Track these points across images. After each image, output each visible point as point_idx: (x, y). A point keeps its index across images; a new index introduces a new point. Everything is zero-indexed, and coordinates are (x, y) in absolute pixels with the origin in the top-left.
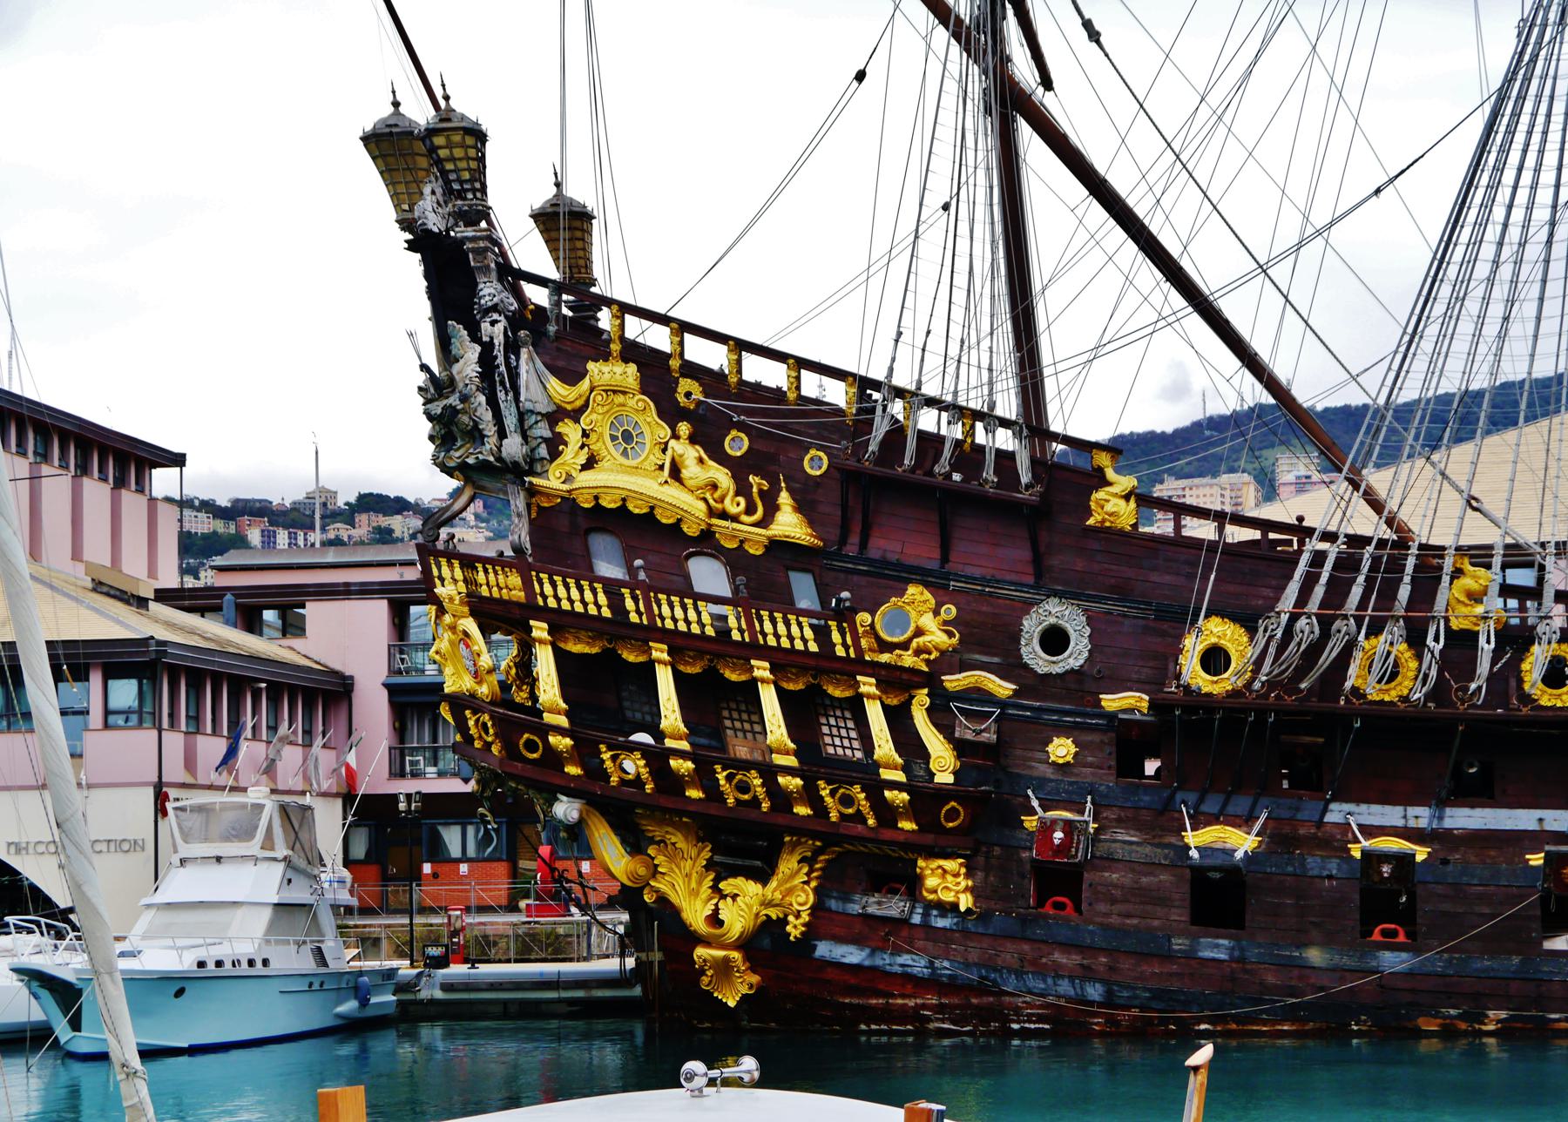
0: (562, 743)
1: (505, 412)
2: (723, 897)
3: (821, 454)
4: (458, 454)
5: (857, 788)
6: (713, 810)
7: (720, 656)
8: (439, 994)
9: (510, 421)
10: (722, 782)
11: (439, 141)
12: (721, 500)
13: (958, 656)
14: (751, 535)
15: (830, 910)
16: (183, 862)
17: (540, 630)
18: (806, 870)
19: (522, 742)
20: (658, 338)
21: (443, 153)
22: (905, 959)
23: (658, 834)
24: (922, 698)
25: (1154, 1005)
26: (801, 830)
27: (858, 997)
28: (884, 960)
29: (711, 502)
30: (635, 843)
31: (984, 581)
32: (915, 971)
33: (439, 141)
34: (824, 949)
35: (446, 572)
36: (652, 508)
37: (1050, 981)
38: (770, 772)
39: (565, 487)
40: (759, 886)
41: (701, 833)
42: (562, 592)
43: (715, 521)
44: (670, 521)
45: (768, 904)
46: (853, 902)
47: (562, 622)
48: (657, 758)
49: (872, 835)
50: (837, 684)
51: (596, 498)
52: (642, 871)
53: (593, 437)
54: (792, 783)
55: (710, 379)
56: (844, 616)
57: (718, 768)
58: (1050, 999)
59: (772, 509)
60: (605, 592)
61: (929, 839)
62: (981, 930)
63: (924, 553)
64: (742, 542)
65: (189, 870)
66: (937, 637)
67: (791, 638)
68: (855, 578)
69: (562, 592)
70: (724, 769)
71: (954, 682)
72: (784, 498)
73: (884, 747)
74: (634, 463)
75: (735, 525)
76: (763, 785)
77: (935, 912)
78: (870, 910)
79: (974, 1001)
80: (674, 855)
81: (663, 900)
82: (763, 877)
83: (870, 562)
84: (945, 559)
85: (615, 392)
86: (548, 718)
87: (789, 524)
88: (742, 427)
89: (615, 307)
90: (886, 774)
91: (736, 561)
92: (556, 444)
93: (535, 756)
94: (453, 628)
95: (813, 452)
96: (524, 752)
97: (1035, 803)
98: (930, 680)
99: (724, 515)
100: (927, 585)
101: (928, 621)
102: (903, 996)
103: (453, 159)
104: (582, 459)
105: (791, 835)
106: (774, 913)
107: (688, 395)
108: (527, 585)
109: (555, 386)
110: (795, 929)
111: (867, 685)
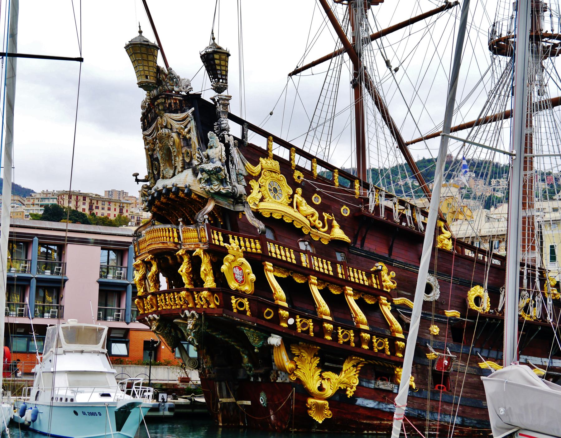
1: (232, 173)
2: (324, 379)
3: (347, 208)
4: (216, 187)
6: (334, 344)
7: (332, 283)
8: (167, 413)
9: (234, 177)
10: (340, 334)
11: (216, 56)
12: (314, 221)
14: (322, 235)
15: (363, 386)
16: (65, 352)
17: (269, 266)
18: (355, 370)
20: (284, 153)
21: (217, 62)
23: (296, 352)
25: (477, 426)
26: (362, 354)
27: (370, 420)
29: (312, 221)
30: (291, 356)
31: (406, 264)
33: (216, 56)
34: (360, 401)
36: (293, 221)
37: (443, 416)
38: (358, 331)
39: (255, 208)
40: (337, 375)
43: (312, 229)
44: (299, 227)
46: (371, 383)
48: (318, 322)
50: (370, 298)
51: (271, 214)
53: (263, 189)
55: (308, 174)
58: (442, 423)
59: (331, 227)
62: (419, 396)
63: (384, 252)
64: (320, 238)
65: (68, 355)
71: (398, 301)
72: (335, 223)
74: (280, 201)
76: (354, 336)
81: (298, 380)
82: (338, 371)
83: (366, 252)
84: (390, 254)
85: (271, 171)
86: (280, 303)
87: (338, 233)
88: (319, 193)
89: (271, 138)
92: (249, 189)
93: (269, 318)
95: (345, 207)
96: (265, 316)
97: (431, 349)
99: (314, 227)
103: (220, 65)
104: (260, 196)
106: (342, 387)
107: (299, 177)
109: (248, 164)
110: (350, 393)
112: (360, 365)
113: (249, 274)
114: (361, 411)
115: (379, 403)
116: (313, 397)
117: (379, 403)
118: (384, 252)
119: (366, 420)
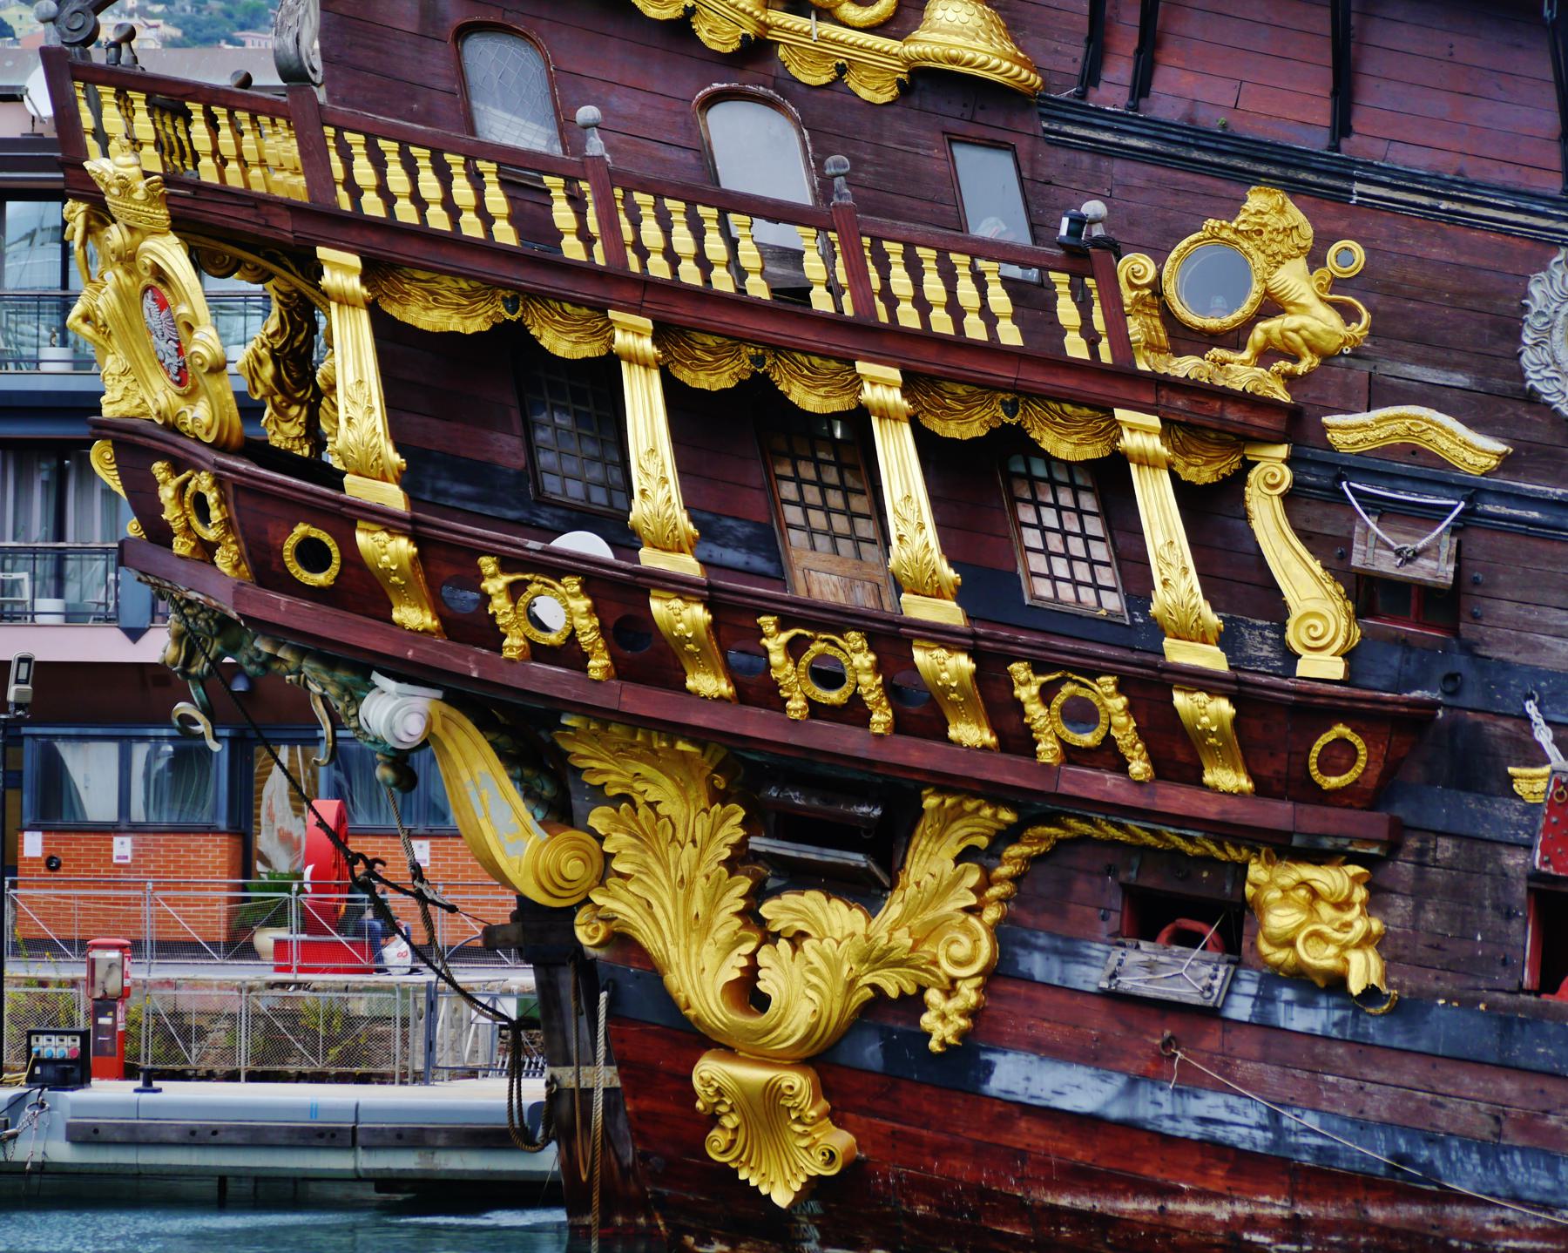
0: (388, 550)
2: (770, 938)
5: (1107, 683)
6: (754, 724)
8: (62, 1152)
10: (777, 658)
13: (1366, 367)
15: (1029, 980)
17: (341, 270)
18: (973, 877)
19: (290, 544)
22: (1210, 1104)
24: (1272, 469)
28: (1159, 1107)
31: (1440, 185)
32: (1234, 1135)
34: (1012, 1075)
35: (113, 119)
38: (892, 639)
41: (721, 783)
42: (397, 179)
44: (670, 13)
45: (880, 959)
46: (1085, 960)
47: (392, 254)
48: (620, 595)
49: (1141, 801)
52: (574, 869)
54: (947, 667)
56: (1088, 258)
57: (768, 623)
60: (504, 184)
61: (1279, 814)
62: (1398, 1041)
63: (1294, 110)
66: (1314, 319)
67: (955, 310)
68: (1117, 167)
69: (397, 179)
70: (782, 627)
73: (1177, 583)
75: (827, 29)
77: (1287, 994)
78: (1128, 983)
79: (1377, 1213)
80: (653, 830)
81: (621, 940)
82: (865, 891)
83: (1159, 129)
84: (1342, 126)
86: (357, 488)
90: (1179, 653)
91: (825, 116)
94: (128, 259)
97: (1544, 735)
98: (1295, 424)
100: (1294, 189)
101: (1294, 280)
102: (1202, 1195)
105: (941, 790)
106: (892, 983)
108: (313, 158)
110: (942, 1024)
111: (1140, 433)
112: (1014, 851)
113: (190, 328)
114: (1026, 1134)
115: (1133, 1083)
116: (727, 1050)
117: (1133, 1083)
118: (1294, 110)
119: (1075, 1191)
